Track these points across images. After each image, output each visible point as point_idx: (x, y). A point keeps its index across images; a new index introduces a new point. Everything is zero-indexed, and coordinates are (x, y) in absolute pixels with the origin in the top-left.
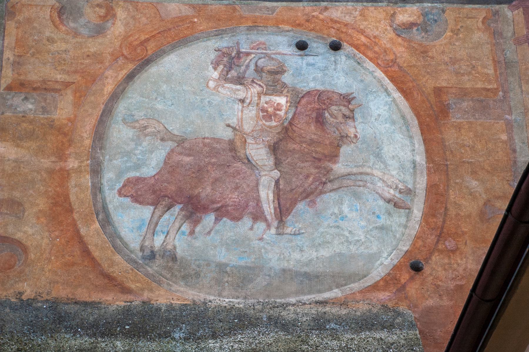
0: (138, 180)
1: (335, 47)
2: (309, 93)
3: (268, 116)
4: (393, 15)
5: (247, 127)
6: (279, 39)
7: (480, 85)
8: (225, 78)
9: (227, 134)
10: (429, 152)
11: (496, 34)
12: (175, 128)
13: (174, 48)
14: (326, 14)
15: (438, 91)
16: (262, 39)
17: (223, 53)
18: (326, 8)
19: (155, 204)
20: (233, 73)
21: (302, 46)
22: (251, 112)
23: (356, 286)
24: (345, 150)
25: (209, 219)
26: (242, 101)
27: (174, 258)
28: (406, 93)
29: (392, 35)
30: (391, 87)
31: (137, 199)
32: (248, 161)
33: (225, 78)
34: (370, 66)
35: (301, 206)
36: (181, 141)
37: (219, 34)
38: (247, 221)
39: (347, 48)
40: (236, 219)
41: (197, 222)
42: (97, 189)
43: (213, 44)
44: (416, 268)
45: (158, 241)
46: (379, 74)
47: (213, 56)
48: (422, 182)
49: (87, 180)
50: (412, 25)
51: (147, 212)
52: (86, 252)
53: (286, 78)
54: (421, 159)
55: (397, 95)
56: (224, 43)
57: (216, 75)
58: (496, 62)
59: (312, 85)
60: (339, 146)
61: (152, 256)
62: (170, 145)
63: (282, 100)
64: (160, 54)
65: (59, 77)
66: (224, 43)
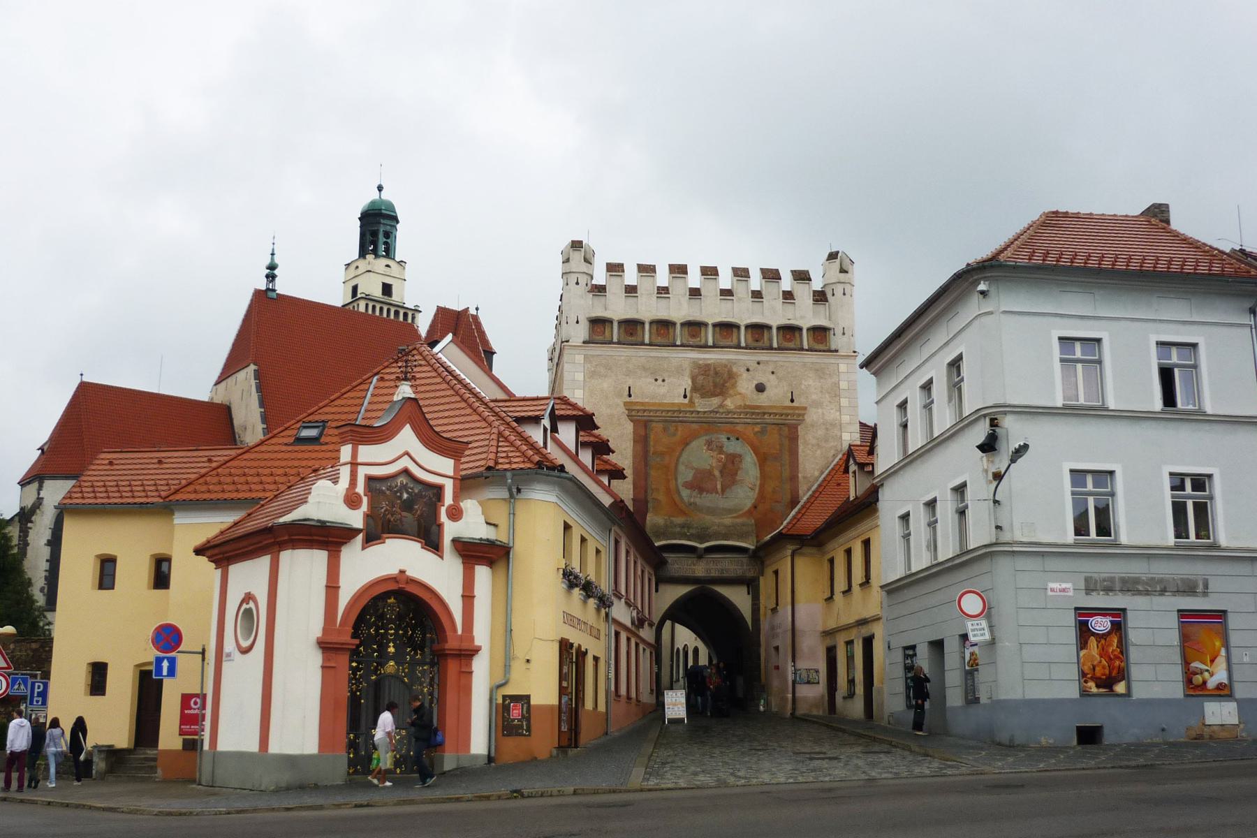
0: (687, 482)
1: (738, 439)
2: (730, 454)
3: (720, 461)
4: (754, 428)
5: (714, 465)
6: (723, 436)
7: (775, 452)
8: (708, 449)
9: (708, 467)
10: (761, 473)
11: (780, 435)
12: (695, 465)
13: (695, 439)
14: (736, 428)
15: (764, 453)
16: (719, 436)
17: (707, 441)
18: (735, 426)
19: (691, 488)
20: (710, 448)
21: (728, 439)
22: (714, 461)
23: (741, 512)
24: (739, 472)
25: (705, 493)
26: (712, 456)
27: (696, 505)
28: (756, 454)
29: (752, 435)
30: (752, 452)
31: (686, 488)
32: (714, 476)
33: (708, 449)
34: (747, 445)
35: (728, 490)
36: (697, 469)
37: (706, 435)
38: (714, 494)
39: (740, 440)
40: (712, 493)
41: (701, 494)
42: (677, 485)
43: (704, 438)
44: (755, 507)
45: (692, 500)
46: (749, 448)
47: (704, 442)
48: (758, 483)
49: (674, 481)
50: (758, 432)
51: (688, 491)
52: (675, 503)
53: (724, 449)
54: (759, 475)
55: (753, 455)
56: (707, 438)
57: (705, 448)
58: (780, 444)
59: (732, 452)
60: (737, 471)
61: (691, 504)
62: (694, 471)
63: (723, 456)
64: (691, 442)
65: (664, 450)
66: (707, 438)
